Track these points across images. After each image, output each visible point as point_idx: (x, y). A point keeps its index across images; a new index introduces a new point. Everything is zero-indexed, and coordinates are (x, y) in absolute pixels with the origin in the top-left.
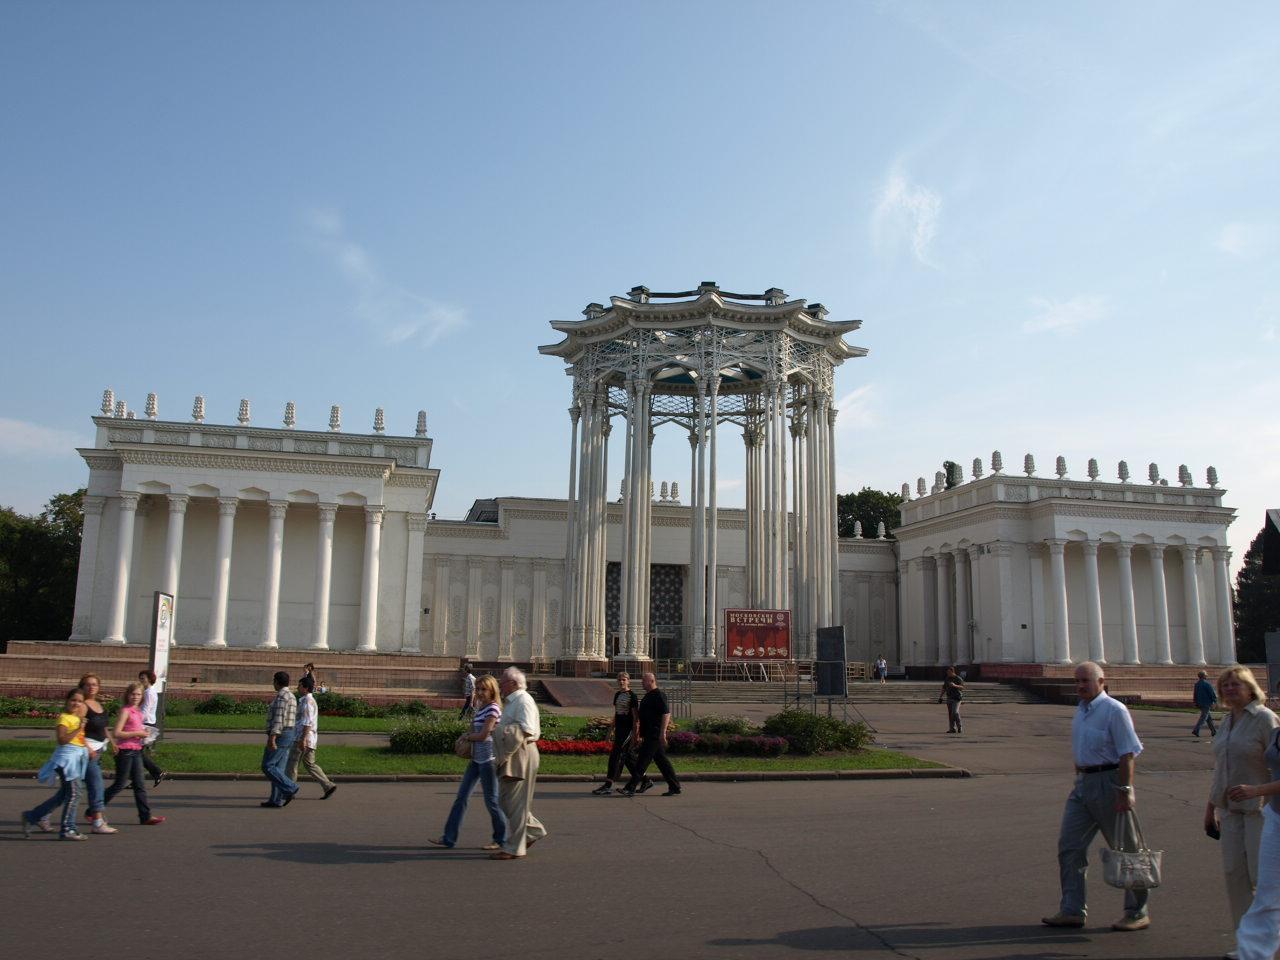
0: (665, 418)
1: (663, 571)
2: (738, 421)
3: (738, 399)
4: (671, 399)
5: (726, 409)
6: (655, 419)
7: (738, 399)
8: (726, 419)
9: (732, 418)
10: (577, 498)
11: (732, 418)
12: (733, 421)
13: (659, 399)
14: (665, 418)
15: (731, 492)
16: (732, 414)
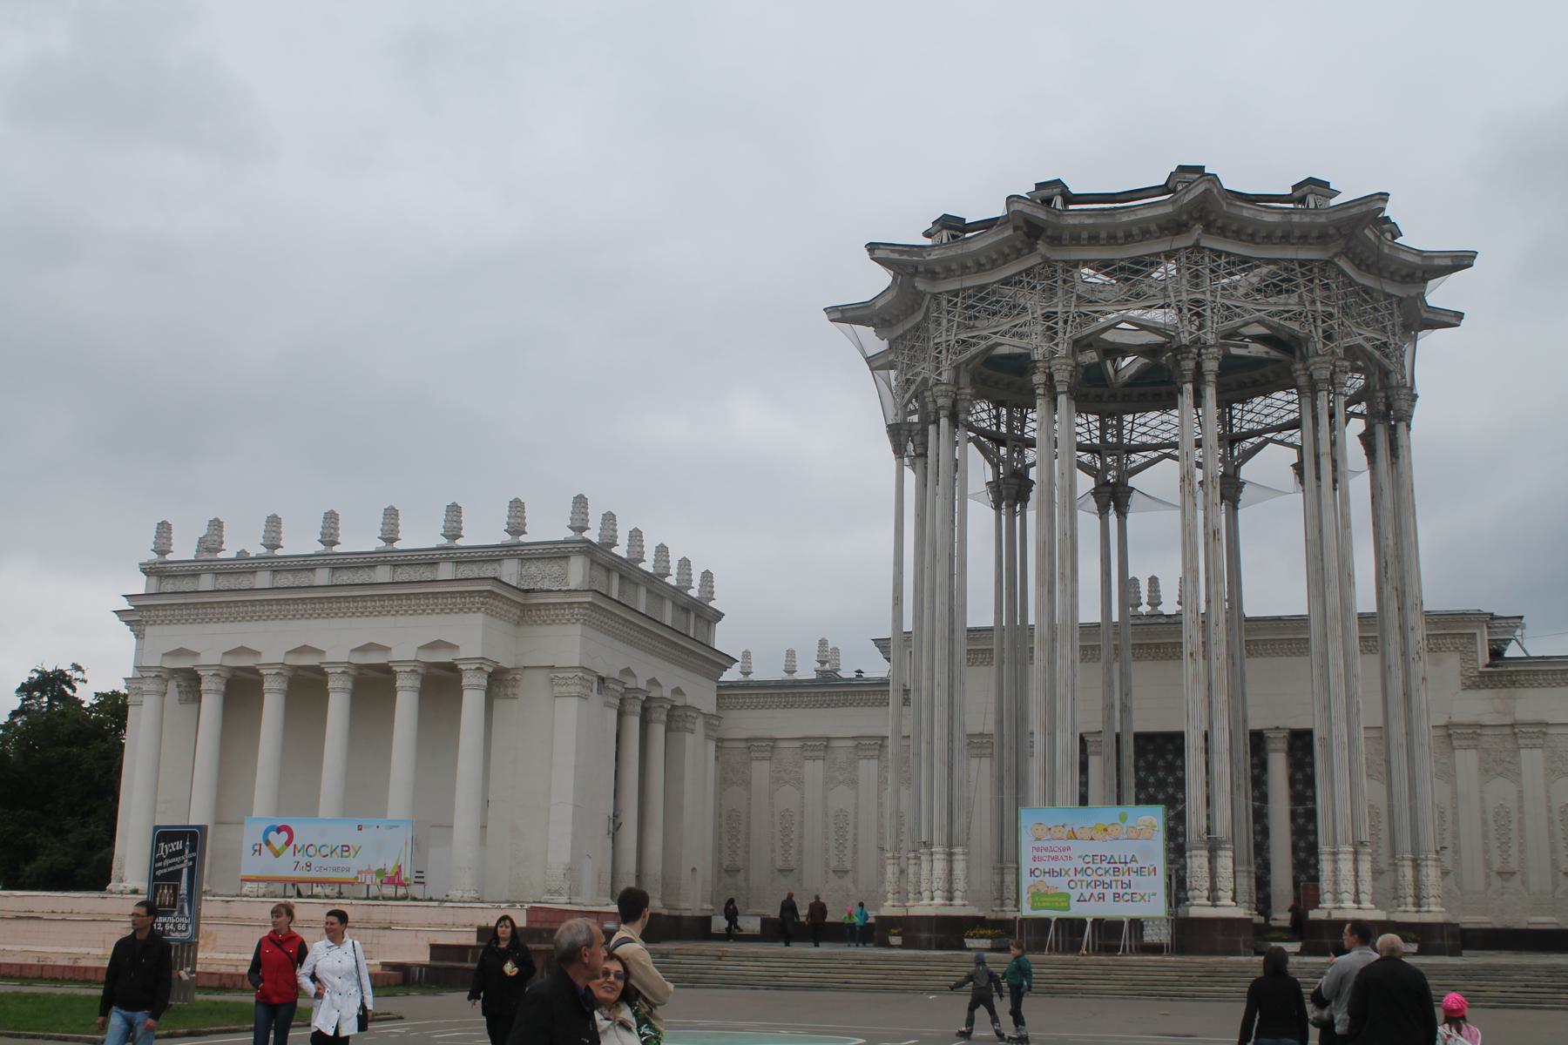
0: (1155, 455)
1: (1151, 747)
2: (1290, 440)
3: (1290, 397)
4: (1165, 417)
5: (1269, 420)
6: (1137, 458)
7: (1290, 397)
8: (1271, 440)
9: (1279, 437)
10: (1115, 618)
11: (1279, 437)
12: (1281, 442)
13: (1142, 420)
14: (1155, 455)
15: (1275, 584)
16: (1279, 429)
